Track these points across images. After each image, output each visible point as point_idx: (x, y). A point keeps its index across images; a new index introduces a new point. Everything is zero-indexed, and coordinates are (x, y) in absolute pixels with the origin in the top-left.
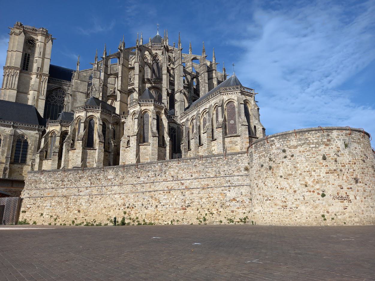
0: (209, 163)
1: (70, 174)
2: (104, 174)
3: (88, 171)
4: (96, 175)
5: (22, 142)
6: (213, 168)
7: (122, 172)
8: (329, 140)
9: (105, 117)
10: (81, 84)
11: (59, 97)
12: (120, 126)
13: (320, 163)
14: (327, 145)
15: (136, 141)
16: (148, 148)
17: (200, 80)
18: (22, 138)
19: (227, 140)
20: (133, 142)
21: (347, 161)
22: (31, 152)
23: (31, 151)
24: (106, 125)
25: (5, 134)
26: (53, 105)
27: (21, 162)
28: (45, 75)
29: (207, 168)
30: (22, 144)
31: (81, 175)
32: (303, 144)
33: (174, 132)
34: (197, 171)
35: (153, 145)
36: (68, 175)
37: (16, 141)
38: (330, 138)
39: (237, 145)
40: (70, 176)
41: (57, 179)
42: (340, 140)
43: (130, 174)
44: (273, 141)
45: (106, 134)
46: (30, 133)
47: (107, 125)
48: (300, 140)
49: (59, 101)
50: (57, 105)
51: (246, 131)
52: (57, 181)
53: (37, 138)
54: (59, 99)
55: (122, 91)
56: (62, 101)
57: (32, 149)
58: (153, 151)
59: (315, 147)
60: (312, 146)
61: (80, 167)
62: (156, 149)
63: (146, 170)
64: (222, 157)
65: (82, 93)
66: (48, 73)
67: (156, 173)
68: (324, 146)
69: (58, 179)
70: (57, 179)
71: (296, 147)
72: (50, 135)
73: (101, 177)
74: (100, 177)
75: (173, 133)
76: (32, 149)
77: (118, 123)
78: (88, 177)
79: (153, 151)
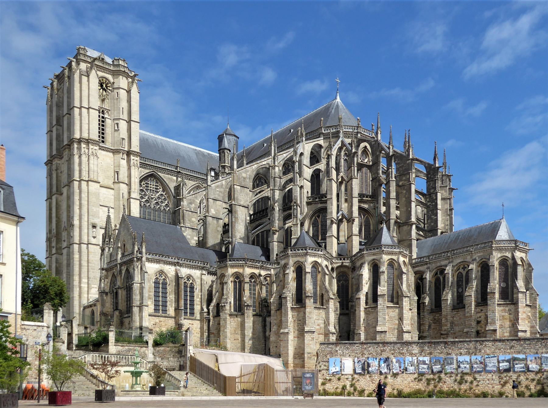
0: (527, 344)
1: (370, 346)
4: (399, 349)
5: (188, 286)
6: (532, 350)
7: (428, 348)
10: (241, 192)
11: (150, 192)
25: (171, 276)
28: (136, 154)
34: (515, 352)
36: (368, 348)
40: (370, 349)
41: (355, 352)
43: (438, 349)
49: (152, 198)
52: (357, 353)
54: (152, 195)
63: (458, 347)
67: (470, 351)
69: (357, 352)
70: (355, 352)
73: (405, 351)
74: (403, 351)
78: (390, 350)
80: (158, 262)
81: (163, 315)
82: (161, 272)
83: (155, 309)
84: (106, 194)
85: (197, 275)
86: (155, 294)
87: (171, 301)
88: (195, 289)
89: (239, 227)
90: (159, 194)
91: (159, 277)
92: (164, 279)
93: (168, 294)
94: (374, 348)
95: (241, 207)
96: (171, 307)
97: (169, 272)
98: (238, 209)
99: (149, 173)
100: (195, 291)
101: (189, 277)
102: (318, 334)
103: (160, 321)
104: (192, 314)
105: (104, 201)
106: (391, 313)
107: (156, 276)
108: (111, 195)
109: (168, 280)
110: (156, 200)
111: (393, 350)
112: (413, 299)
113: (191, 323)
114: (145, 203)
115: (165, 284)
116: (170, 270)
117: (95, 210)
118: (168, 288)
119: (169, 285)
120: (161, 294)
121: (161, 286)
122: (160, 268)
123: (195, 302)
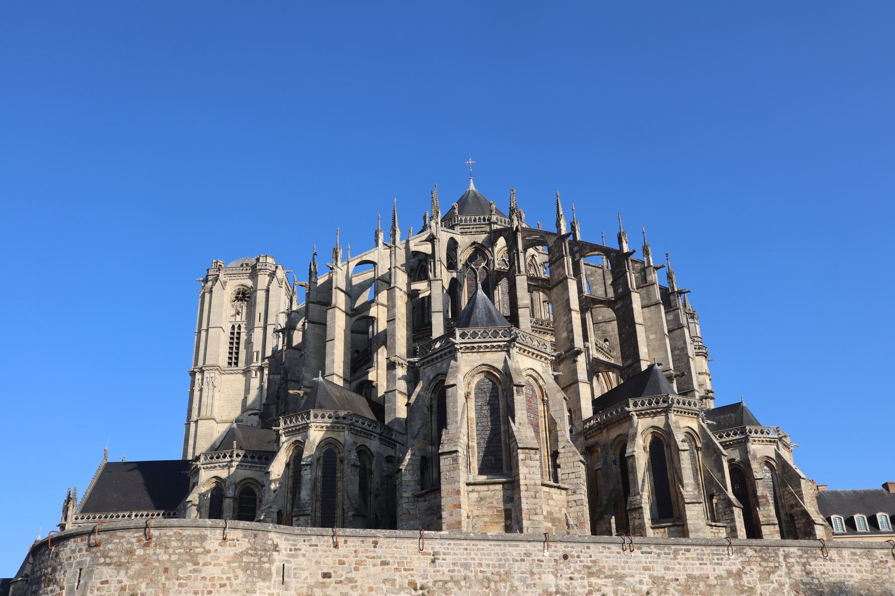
24: (255, 495)
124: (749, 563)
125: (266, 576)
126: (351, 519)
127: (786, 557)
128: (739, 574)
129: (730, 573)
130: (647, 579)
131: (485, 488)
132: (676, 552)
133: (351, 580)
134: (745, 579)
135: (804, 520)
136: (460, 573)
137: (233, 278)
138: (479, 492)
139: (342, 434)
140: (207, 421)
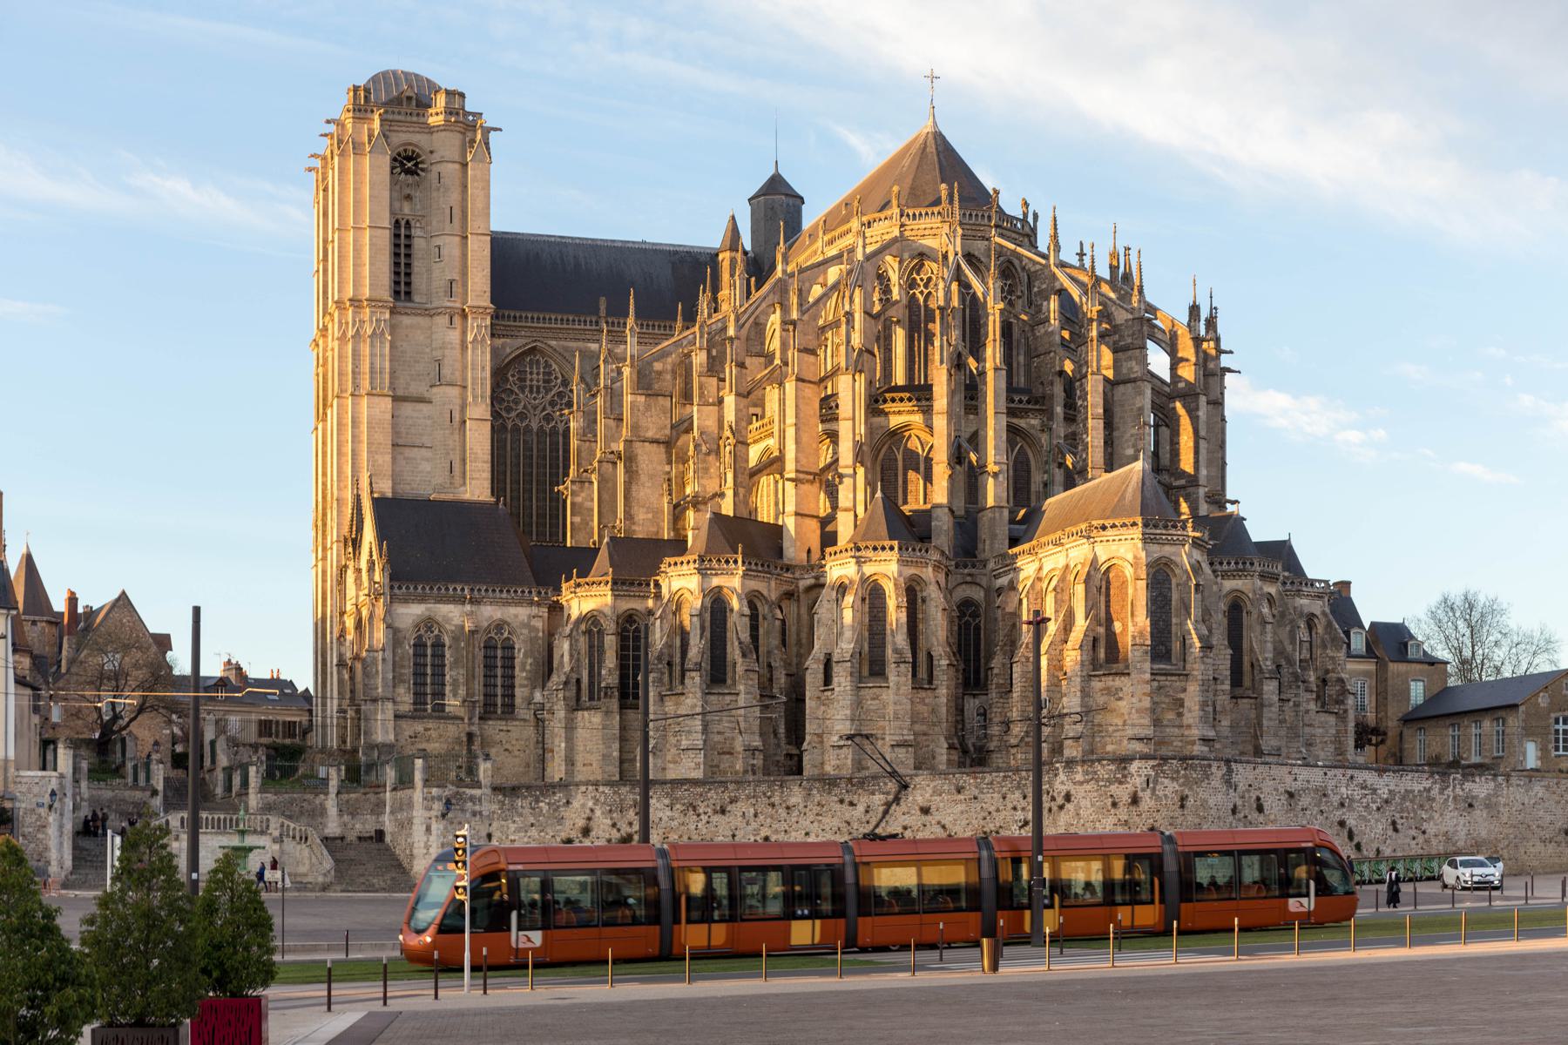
1: (710, 789)
2: (782, 792)
3: (749, 786)
4: (764, 794)
7: (819, 791)
8: (1125, 776)
9: (754, 584)
10: (648, 408)
11: (531, 391)
12: (798, 600)
13: (1108, 811)
14: (1121, 783)
15: (849, 678)
16: (884, 697)
17: (1079, 398)
18: (496, 634)
19: (1097, 685)
20: (842, 679)
21: (1146, 807)
22: (526, 678)
23: (524, 674)
25: (453, 628)
26: (516, 429)
27: (503, 713)
29: (982, 793)
30: (499, 653)
31: (733, 794)
32: (1091, 779)
33: (975, 615)
35: (898, 689)
37: (482, 645)
38: (1126, 772)
39: (1120, 699)
42: (1140, 776)
44: (1057, 769)
45: (761, 637)
46: (516, 616)
47: (760, 609)
48: (1087, 773)
49: (535, 408)
50: (528, 429)
51: (1145, 661)
53: (538, 630)
54: (535, 399)
55: (801, 476)
56: (544, 409)
57: (528, 667)
58: (898, 707)
59: (1105, 786)
60: (1101, 783)
61: (701, 747)
62: (905, 701)
64: (1010, 774)
65: (655, 445)
66: (486, 301)
68: (1116, 785)
71: (1081, 783)
72: (583, 627)
75: (971, 620)
76: (528, 667)
77: (793, 595)
79: (898, 707)
80: (422, 599)
81: (437, 714)
82: (429, 623)
83: (415, 703)
84: (412, 418)
85: (521, 618)
86: (415, 669)
87: (455, 683)
88: (516, 651)
89: (642, 494)
90: (553, 393)
91: (426, 632)
92: (436, 636)
93: (447, 669)
94: (717, 794)
95: (647, 444)
96: (455, 695)
97: (448, 620)
98: (639, 451)
99: (524, 346)
100: (516, 655)
101: (500, 626)
102: (719, 754)
103: (426, 730)
104: (510, 708)
105: (407, 433)
106: (869, 702)
107: (419, 630)
108: (425, 418)
109: (446, 638)
110: (544, 409)
111: (754, 797)
112: (939, 666)
113: (505, 728)
114: (517, 421)
115: (438, 645)
116: (453, 615)
117: (380, 462)
118: (448, 656)
119: (450, 647)
120: (429, 671)
121: (429, 651)
122: (427, 613)
123: (517, 682)
124: (1435, 783)
125: (1231, 787)
126: (945, 668)
127: (1454, 779)
128: (1428, 790)
129: (1425, 788)
130: (1386, 791)
131: (1163, 678)
132: (1402, 776)
133: (1260, 788)
134: (1432, 792)
135: (1338, 688)
136: (1306, 785)
137: (396, 128)
138: (1159, 681)
139: (924, 570)
140: (380, 398)
